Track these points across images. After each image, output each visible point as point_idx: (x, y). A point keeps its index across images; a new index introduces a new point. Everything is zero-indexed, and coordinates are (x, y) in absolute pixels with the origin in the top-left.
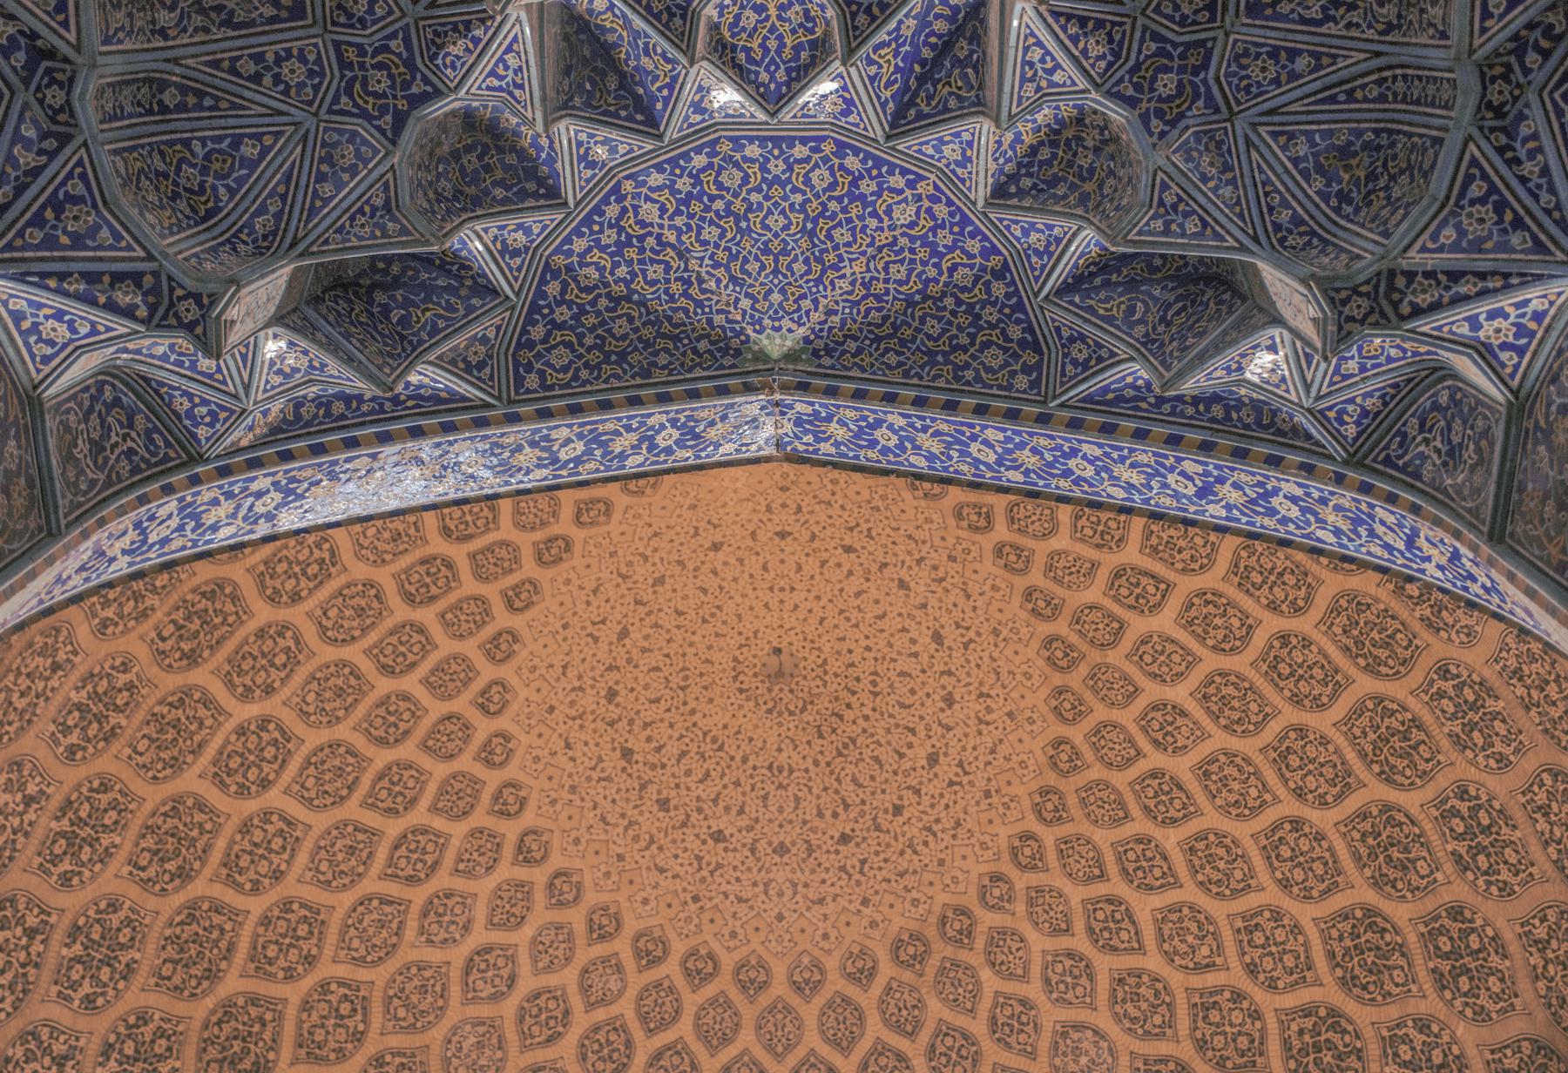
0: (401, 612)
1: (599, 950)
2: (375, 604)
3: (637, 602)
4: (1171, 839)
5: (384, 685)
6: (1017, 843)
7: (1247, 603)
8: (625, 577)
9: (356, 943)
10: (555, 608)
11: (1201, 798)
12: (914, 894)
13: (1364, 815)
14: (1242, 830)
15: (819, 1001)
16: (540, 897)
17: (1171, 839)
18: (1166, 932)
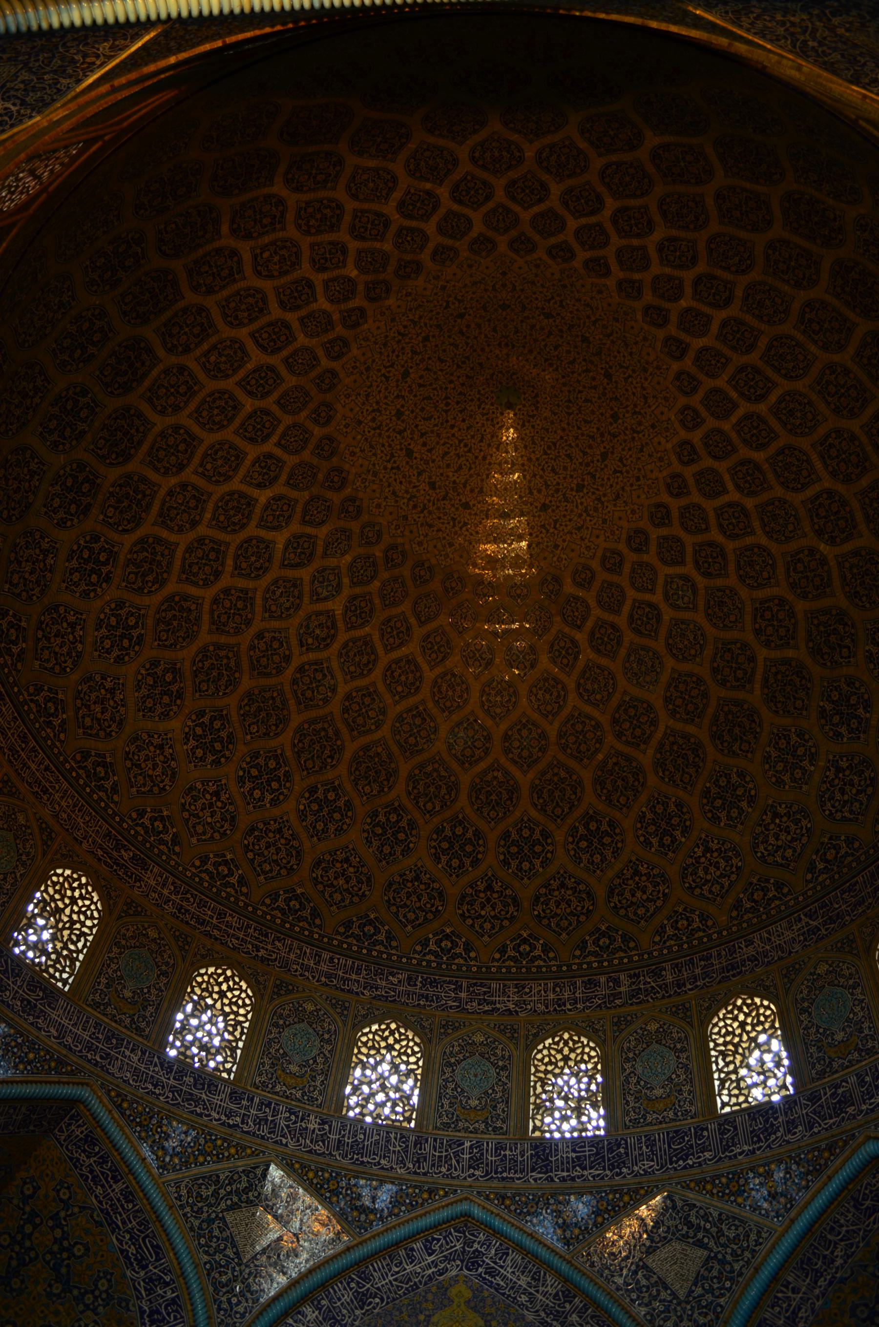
0: (730, 546)
1: (637, 276)
2: (742, 563)
3: (593, 476)
4: (249, 405)
5: (750, 503)
6: (344, 350)
7: (241, 583)
8: (599, 500)
9: (801, 357)
10: (643, 496)
11: (238, 441)
12: (409, 299)
13: (149, 506)
14: (210, 438)
15: (474, 234)
16: (674, 318)
17: (249, 405)
18: (239, 353)
